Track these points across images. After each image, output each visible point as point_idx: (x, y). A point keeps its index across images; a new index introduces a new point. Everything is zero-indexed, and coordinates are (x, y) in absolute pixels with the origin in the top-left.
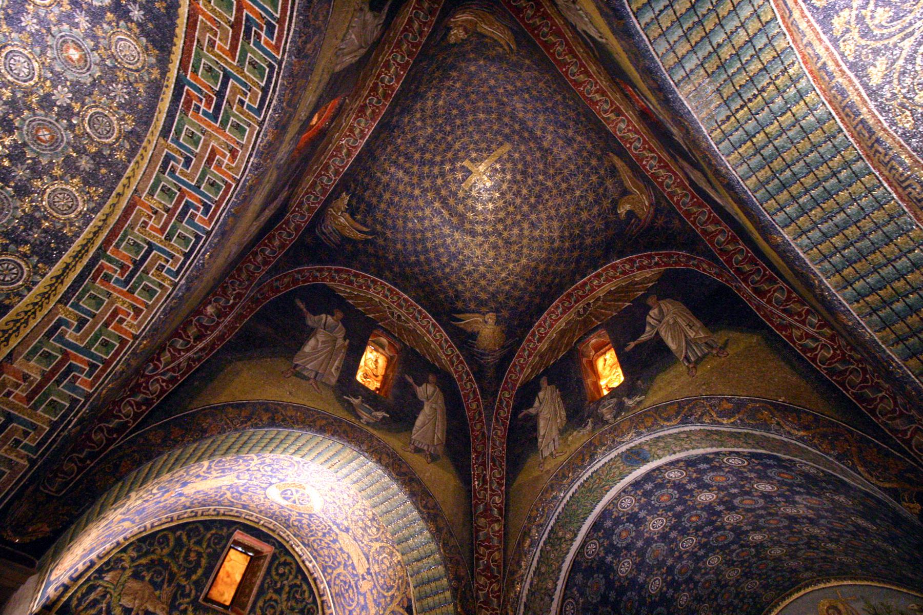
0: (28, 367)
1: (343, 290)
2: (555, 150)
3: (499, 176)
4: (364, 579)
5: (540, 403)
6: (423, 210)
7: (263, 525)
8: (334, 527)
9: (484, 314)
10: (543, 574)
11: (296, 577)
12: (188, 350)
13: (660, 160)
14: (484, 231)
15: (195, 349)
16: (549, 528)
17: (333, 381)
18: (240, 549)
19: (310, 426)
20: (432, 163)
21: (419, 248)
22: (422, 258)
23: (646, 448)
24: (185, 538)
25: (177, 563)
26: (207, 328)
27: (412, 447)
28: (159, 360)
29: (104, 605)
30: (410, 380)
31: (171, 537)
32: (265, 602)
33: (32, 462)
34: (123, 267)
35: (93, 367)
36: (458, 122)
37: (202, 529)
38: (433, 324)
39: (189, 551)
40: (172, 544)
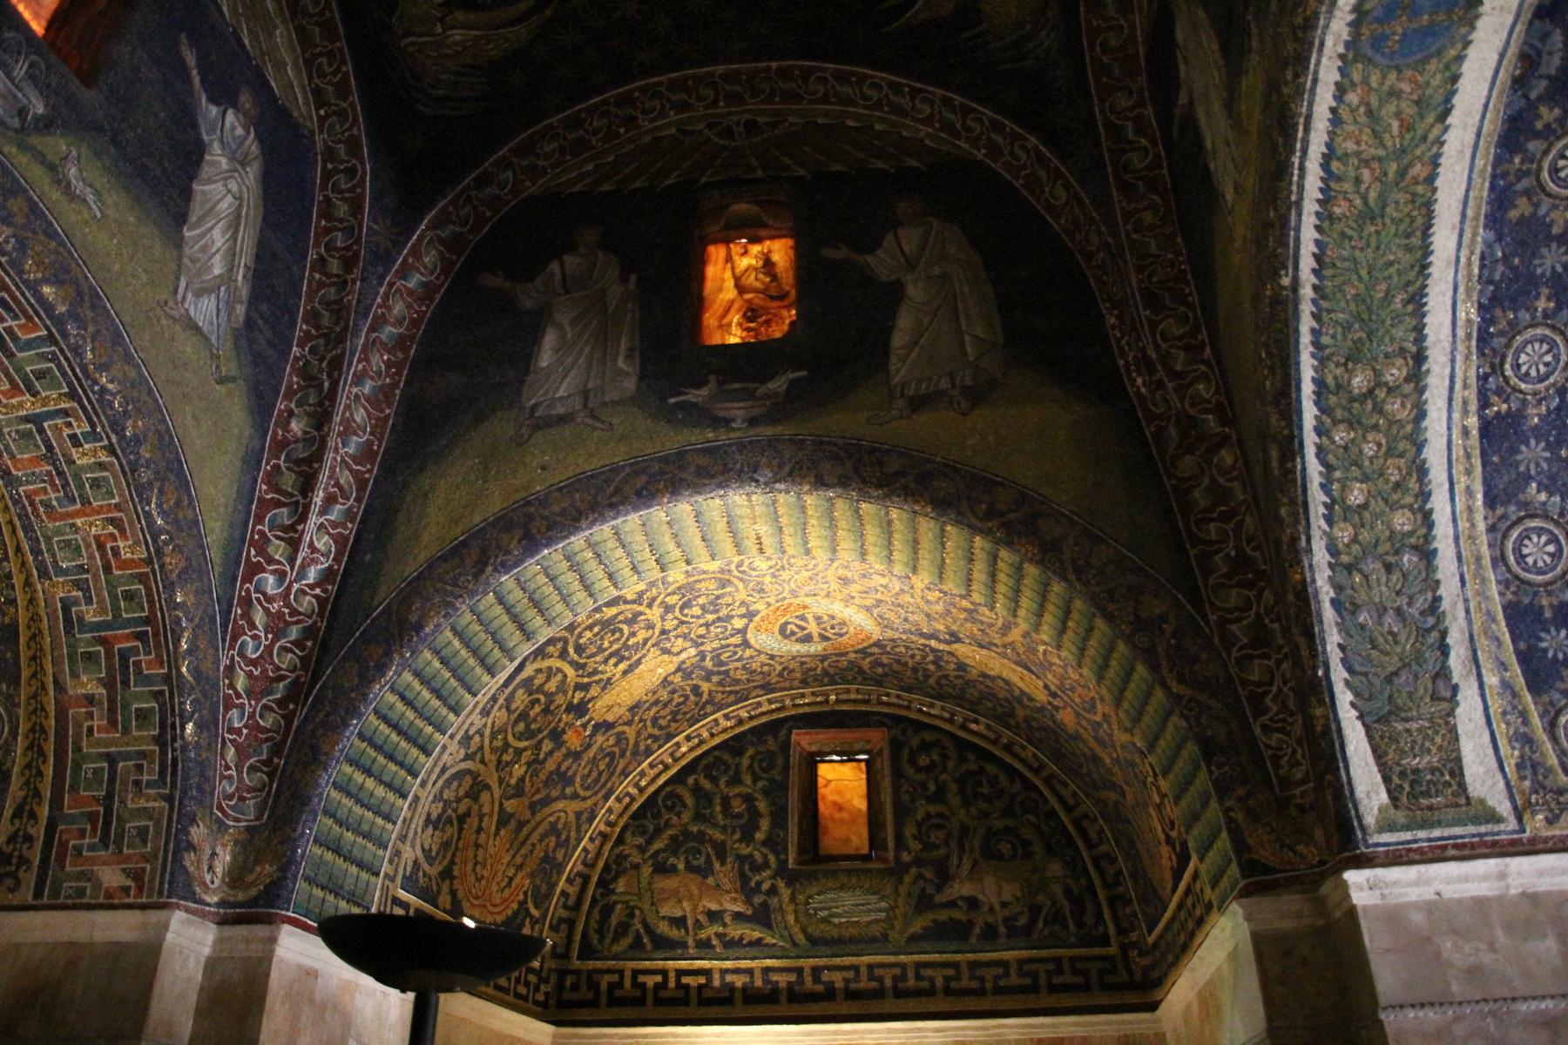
0: (84, 685)
4: (1057, 708)
5: (1186, 60)
7: (838, 701)
8: (933, 643)
10: (1365, 506)
11: (962, 759)
12: (303, 518)
16: (1307, 388)
17: (630, 384)
18: (835, 758)
19: (612, 506)
24: (706, 784)
25: (715, 825)
26: (309, 461)
27: (900, 403)
28: (271, 561)
29: (639, 926)
30: (841, 253)
31: (680, 790)
32: (919, 825)
33: (169, 799)
35: (141, 636)
37: (726, 757)
38: (838, 76)
39: (726, 802)
40: (690, 801)
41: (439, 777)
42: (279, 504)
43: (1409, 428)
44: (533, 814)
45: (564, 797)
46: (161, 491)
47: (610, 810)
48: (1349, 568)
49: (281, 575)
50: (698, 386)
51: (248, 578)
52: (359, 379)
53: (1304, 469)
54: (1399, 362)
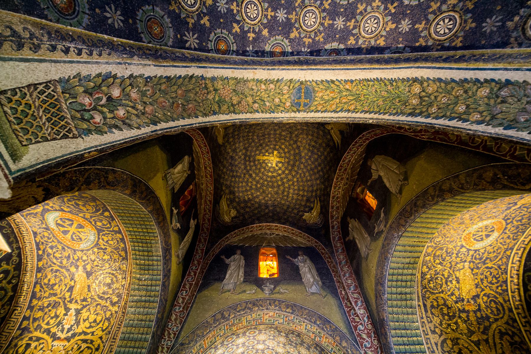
1: (341, 213)
2: (242, 148)
3: (270, 151)
6: (301, 174)
9: (329, 130)
10: (468, 107)
12: (355, 311)
13: (201, 149)
14: (294, 144)
15: (355, 306)
16: (410, 119)
20: (282, 179)
21: (316, 171)
22: (319, 168)
23: (288, 104)
27: (398, 196)
28: (358, 322)
30: (370, 181)
34: (315, 337)
36: (261, 181)
41: (437, 347)
42: (351, 310)
43: (443, 85)
44: (487, 335)
45: (493, 322)
46: (326, 327)
47: (518, 314)
48: (493, 117)
49: (361, 324)
50: (375, 228)
51: (356, 330)
52: (344, 276)
53: (440, 125)
54: (413, 88)
